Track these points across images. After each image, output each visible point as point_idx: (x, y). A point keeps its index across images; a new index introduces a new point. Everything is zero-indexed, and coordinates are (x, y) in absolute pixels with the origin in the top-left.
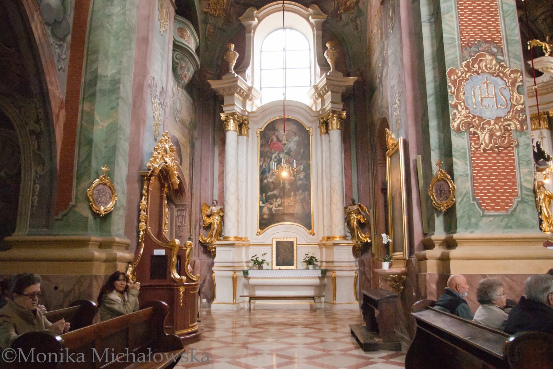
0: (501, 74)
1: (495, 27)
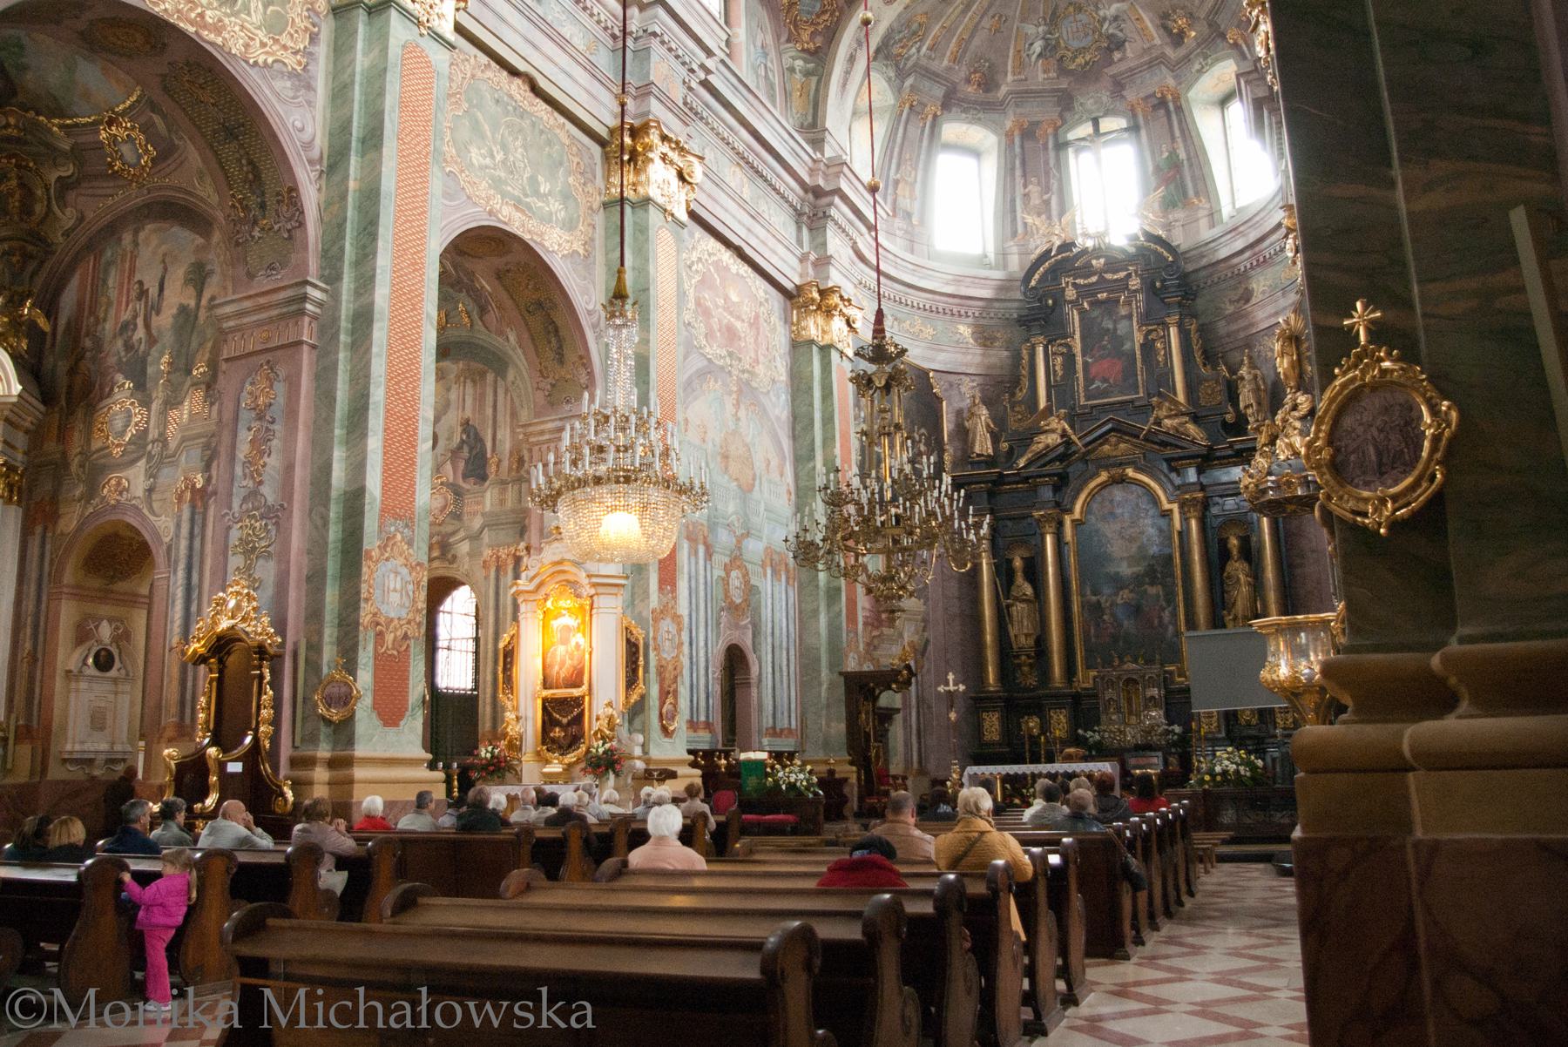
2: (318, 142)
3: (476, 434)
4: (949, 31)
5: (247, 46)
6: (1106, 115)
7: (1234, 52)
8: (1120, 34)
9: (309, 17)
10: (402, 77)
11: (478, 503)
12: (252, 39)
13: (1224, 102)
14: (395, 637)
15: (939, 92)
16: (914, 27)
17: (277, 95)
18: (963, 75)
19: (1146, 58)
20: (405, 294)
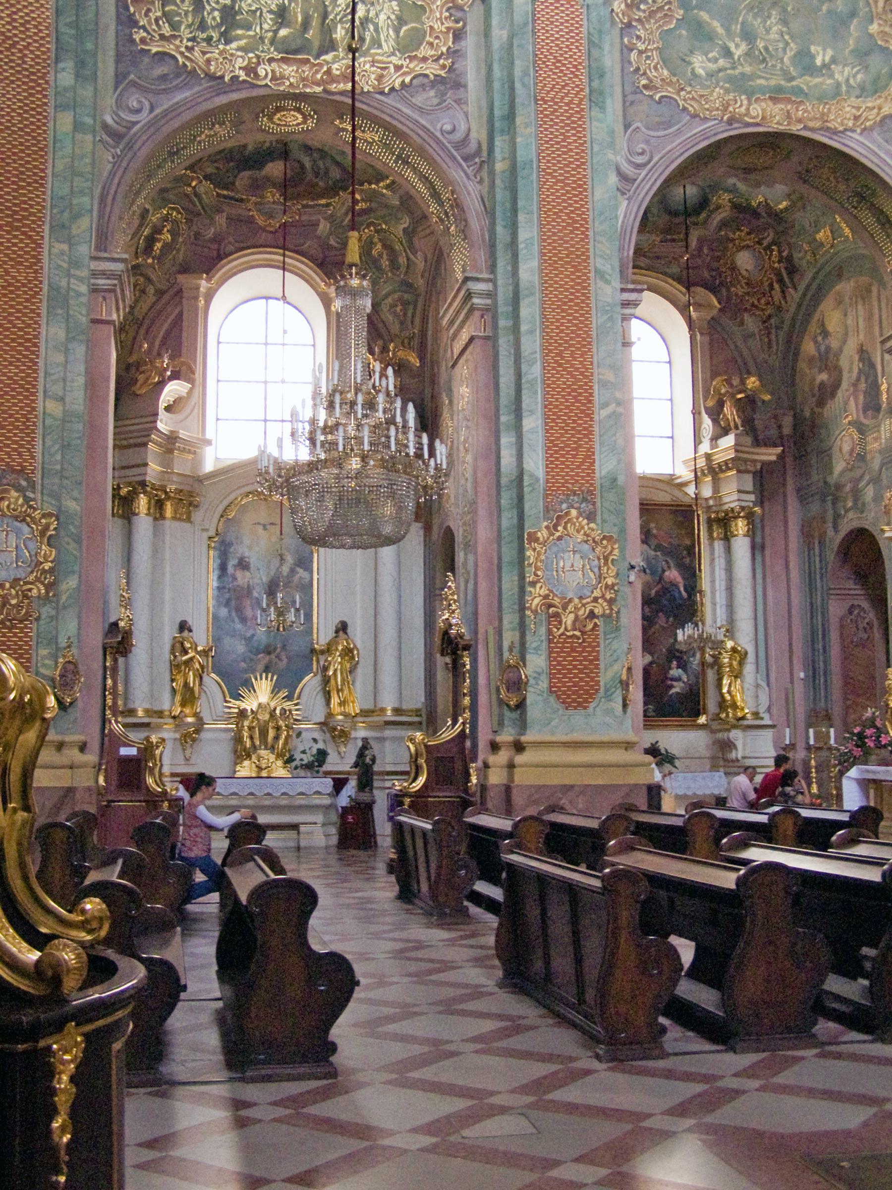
0: (28, 519)
1: (29, 450)
2: (473, 135)
3: (869, 359)
5: (380, 78)
9: (451, 15)
10: (534, 33)
11: (876, 439)
12: (386, 68)
14: (577, 618)
17: (420, 110)
20: (561, 259)
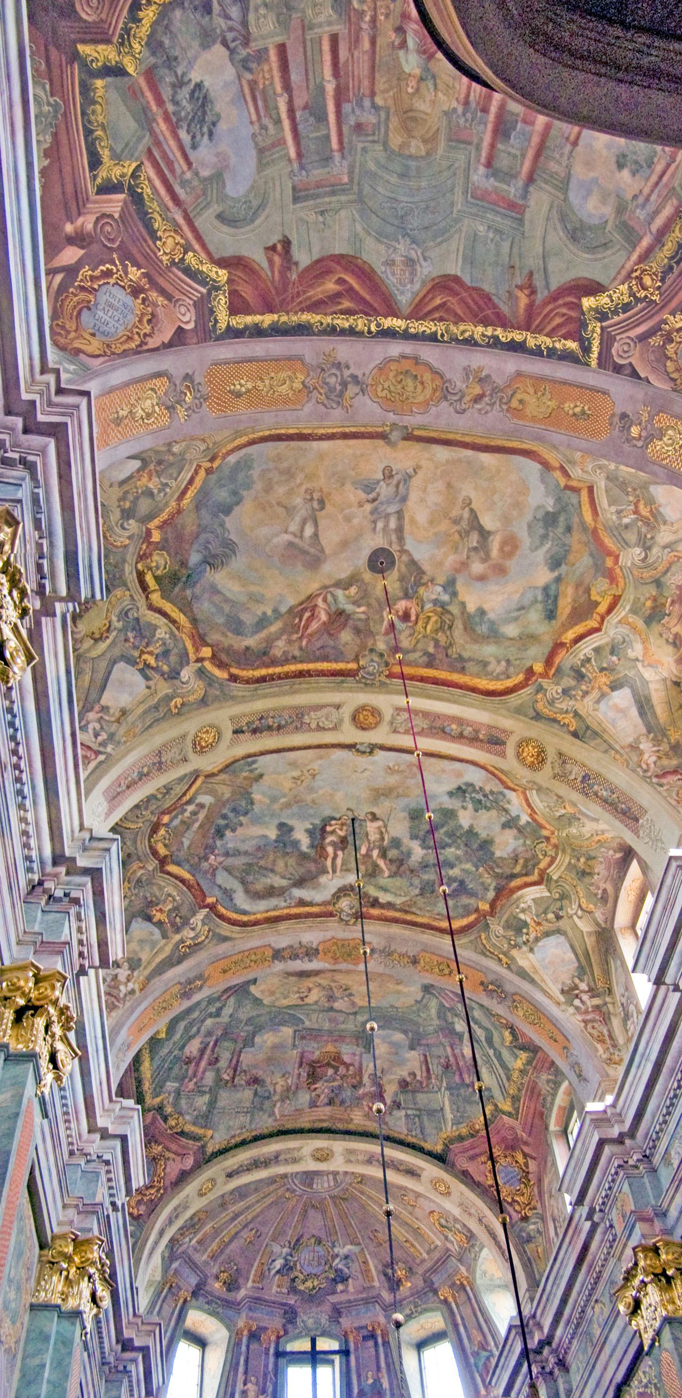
4: (216, 1232)
6: (324, 1334)
7: (444, 1308)
8: (346, 1270)
13: (421, 1346)
15: (194, 1280)
16: (196, 1220)
18: (215, 1270)
19: (364, 1295)
